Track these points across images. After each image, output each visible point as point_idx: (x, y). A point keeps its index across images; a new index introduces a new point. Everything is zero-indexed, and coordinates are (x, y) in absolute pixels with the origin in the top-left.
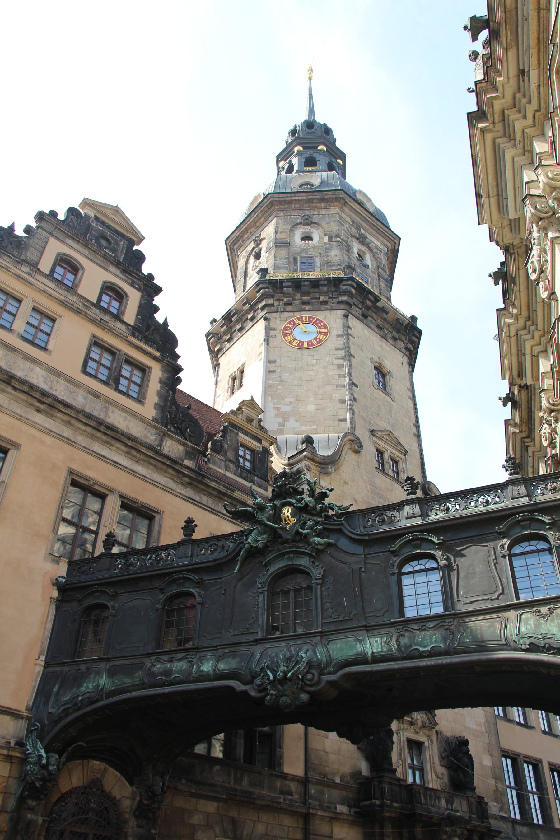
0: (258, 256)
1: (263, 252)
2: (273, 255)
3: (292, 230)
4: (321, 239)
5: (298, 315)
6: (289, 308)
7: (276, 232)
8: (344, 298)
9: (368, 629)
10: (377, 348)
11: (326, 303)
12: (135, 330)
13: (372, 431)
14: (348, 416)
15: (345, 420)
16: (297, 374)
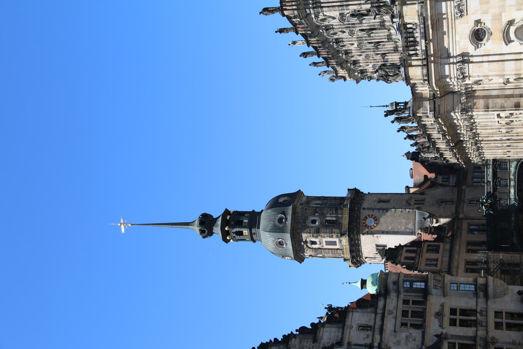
0: (313, 243)
1: (313, 239)
2: (323, 235)
3: (309, 227)
4: (315, 216)
5: (361, 224)
6: (358, 227)
7: (310, 233)
8: (356, 209)
9: (510, 192)
10: (370, 202)
11: (357, 215)
12: (417, 247)
13: (410, 205)
14: (408, 210)
15: (409, 211)
16: (389, 224)
